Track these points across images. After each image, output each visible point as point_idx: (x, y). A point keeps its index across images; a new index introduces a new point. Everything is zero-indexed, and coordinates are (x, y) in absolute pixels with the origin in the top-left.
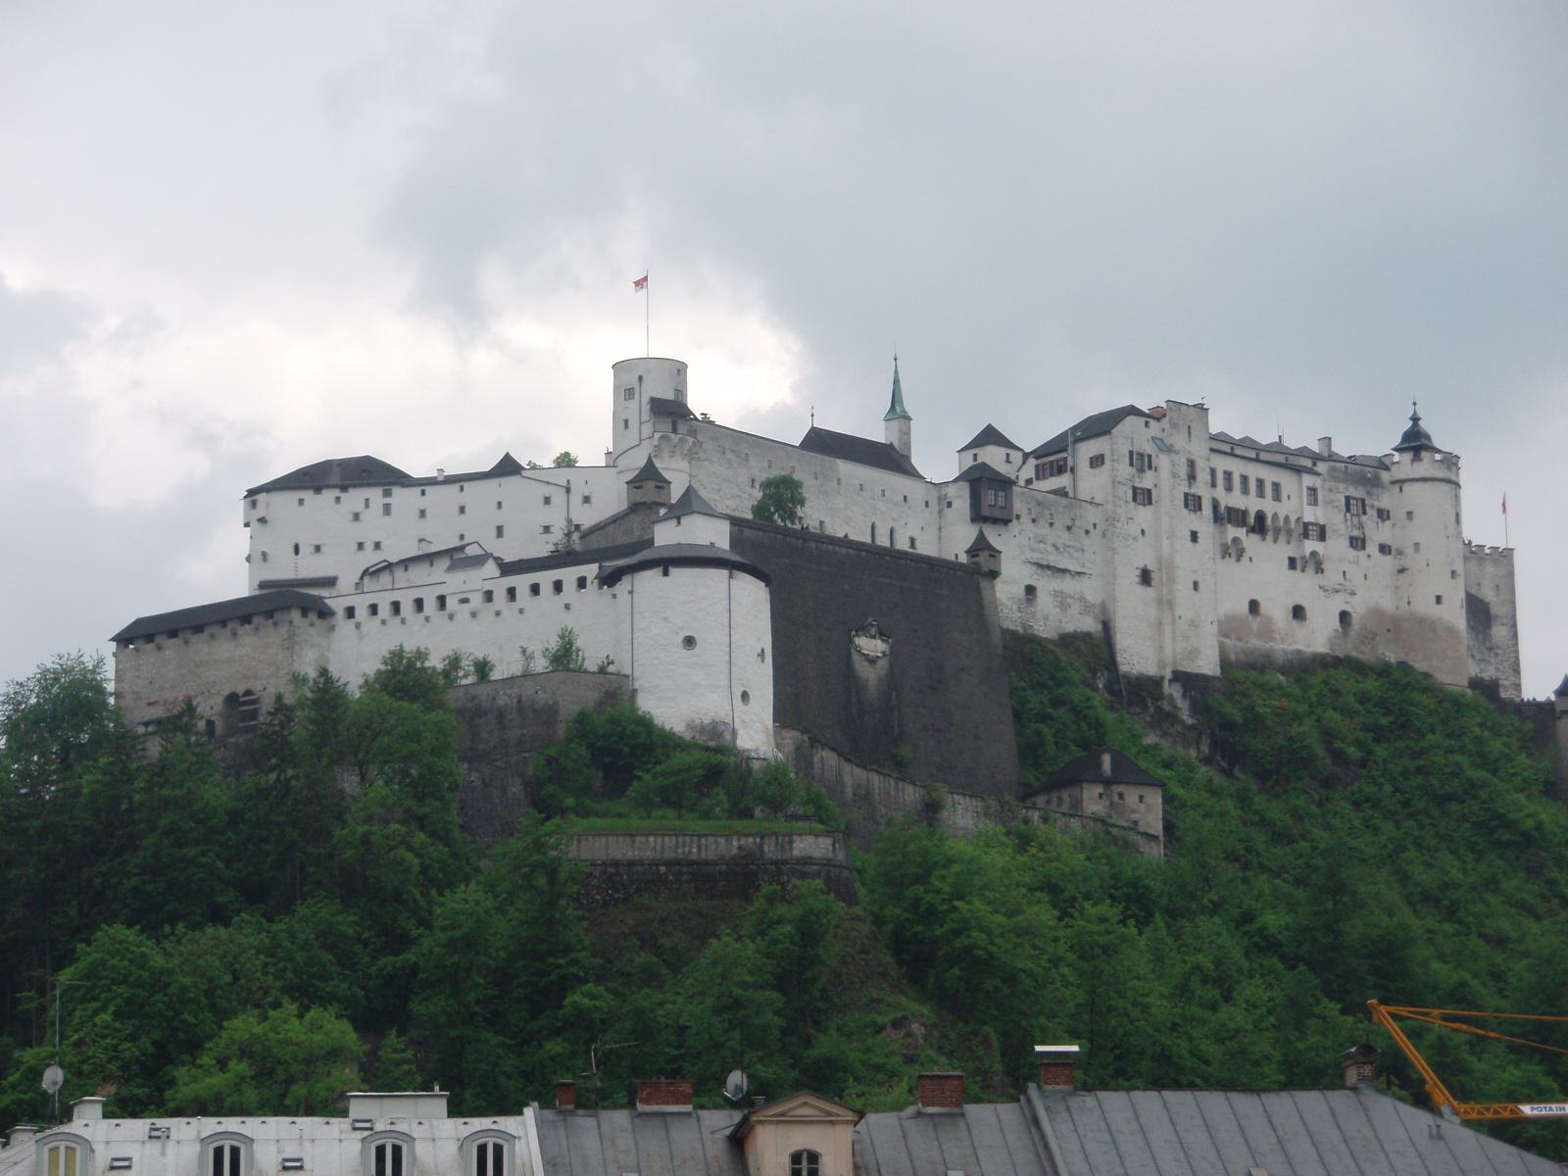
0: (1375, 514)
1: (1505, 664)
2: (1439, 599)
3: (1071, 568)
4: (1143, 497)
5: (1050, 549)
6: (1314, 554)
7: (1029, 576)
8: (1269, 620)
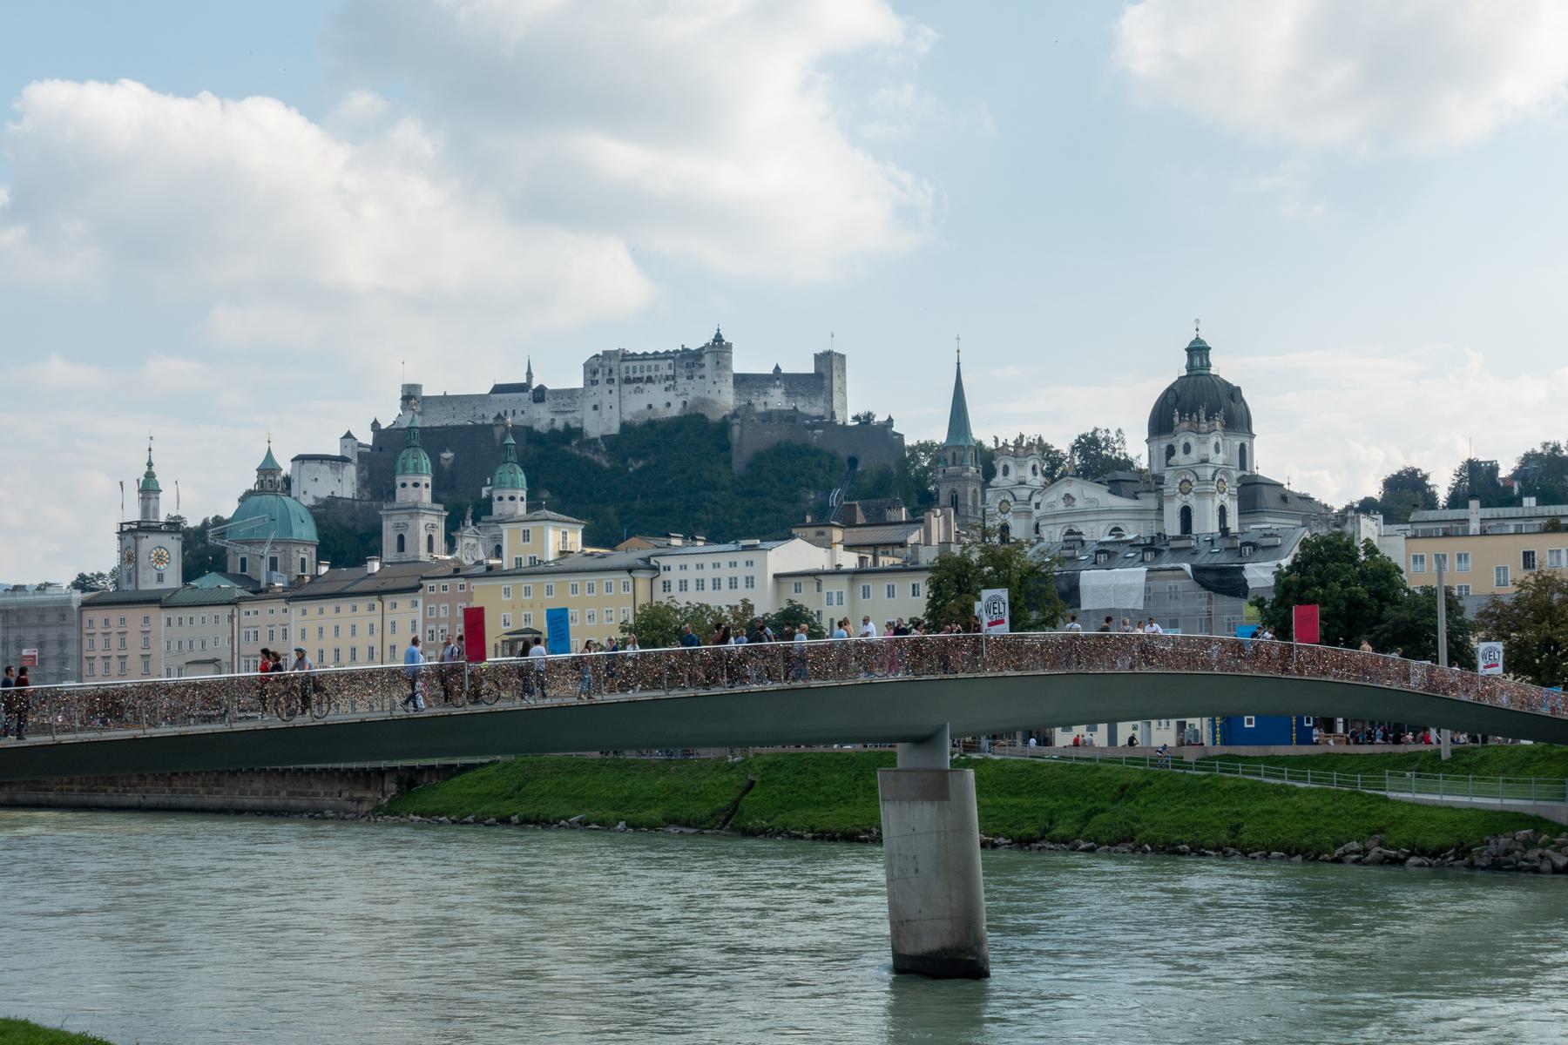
4: (595, 383)
7: (551, 416)
8: (656, 409)
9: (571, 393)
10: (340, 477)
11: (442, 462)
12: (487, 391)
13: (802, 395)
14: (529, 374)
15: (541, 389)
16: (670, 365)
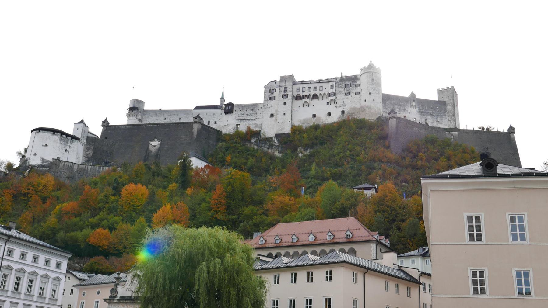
0: (355, 86)
1: (450, 115)
2: (365, 100)
3: (252, 118)
5: (245, 115)
6: (332, 100)
8: (320, 118)
9: (253, 107)
10: (68, 148)
11: (151, 148)
12: (192, 109)
13: (431, 115)
14: (222, 98)
15: (231, 105)
16: (332, 86)
